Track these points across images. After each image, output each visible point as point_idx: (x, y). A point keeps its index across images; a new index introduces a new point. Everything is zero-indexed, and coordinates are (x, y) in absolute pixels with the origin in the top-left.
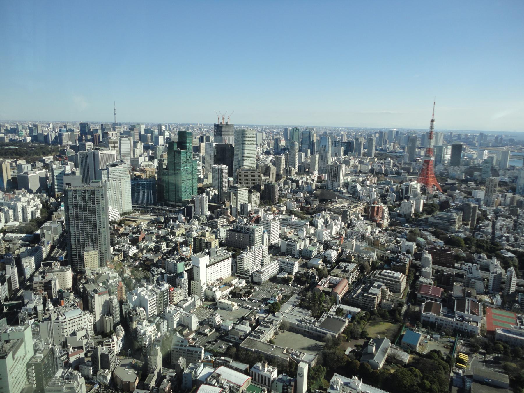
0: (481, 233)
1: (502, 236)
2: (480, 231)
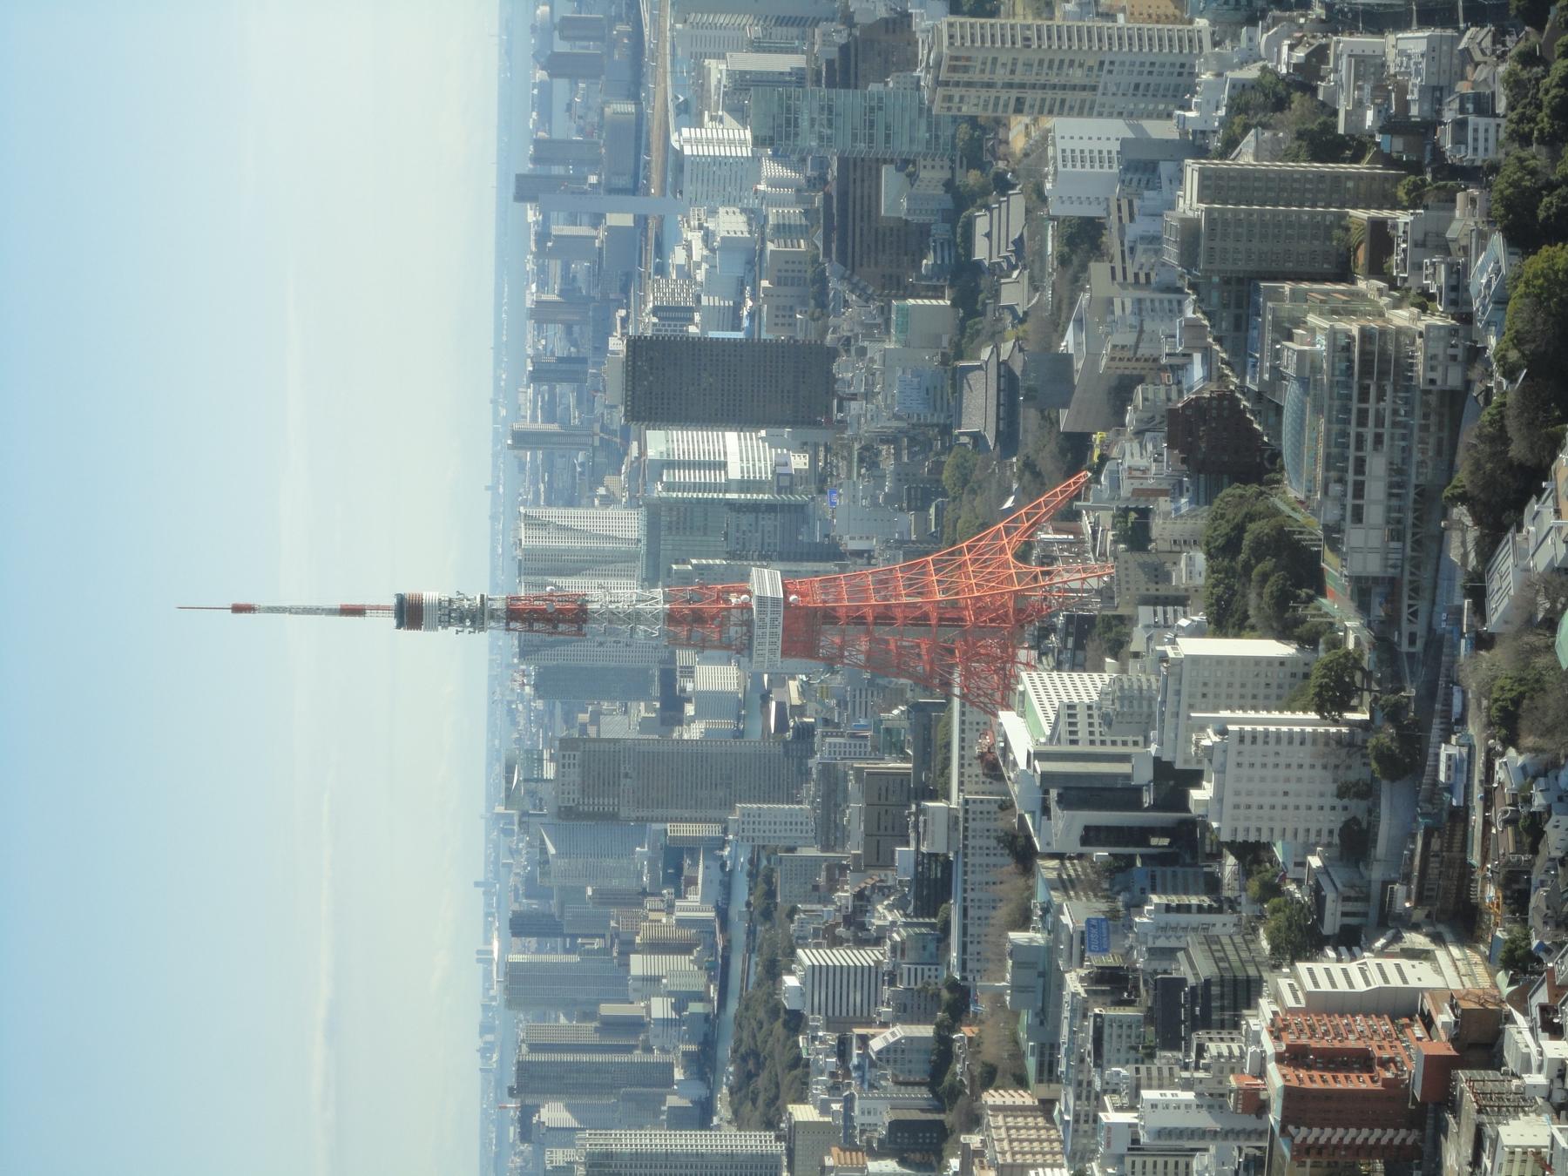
0: (1449, 116)
2: (1429, 126)
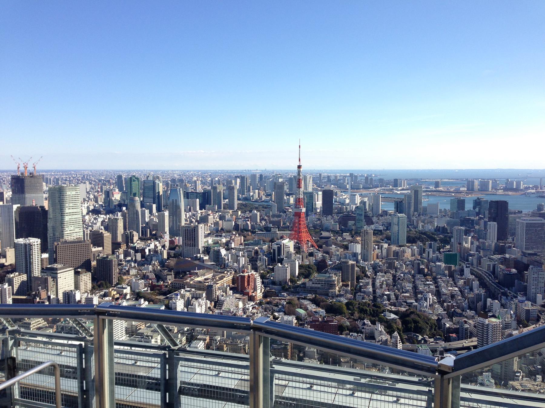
0: (362, 294)
1: (383, 295)
2: (361, 292)
